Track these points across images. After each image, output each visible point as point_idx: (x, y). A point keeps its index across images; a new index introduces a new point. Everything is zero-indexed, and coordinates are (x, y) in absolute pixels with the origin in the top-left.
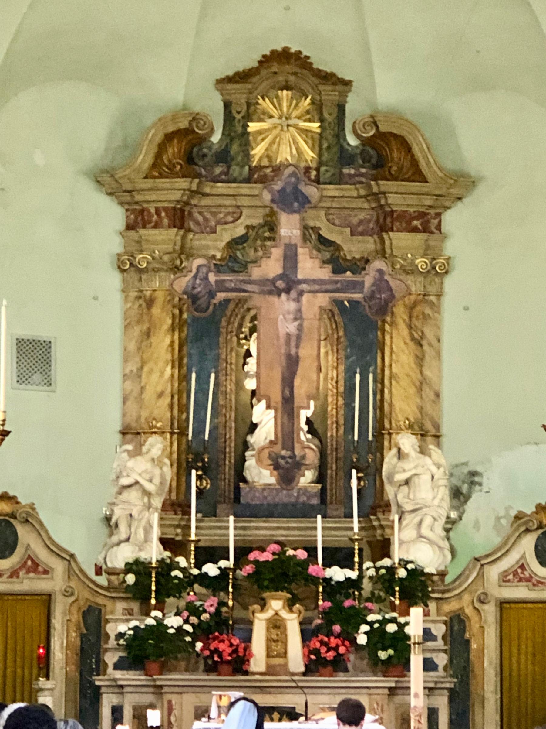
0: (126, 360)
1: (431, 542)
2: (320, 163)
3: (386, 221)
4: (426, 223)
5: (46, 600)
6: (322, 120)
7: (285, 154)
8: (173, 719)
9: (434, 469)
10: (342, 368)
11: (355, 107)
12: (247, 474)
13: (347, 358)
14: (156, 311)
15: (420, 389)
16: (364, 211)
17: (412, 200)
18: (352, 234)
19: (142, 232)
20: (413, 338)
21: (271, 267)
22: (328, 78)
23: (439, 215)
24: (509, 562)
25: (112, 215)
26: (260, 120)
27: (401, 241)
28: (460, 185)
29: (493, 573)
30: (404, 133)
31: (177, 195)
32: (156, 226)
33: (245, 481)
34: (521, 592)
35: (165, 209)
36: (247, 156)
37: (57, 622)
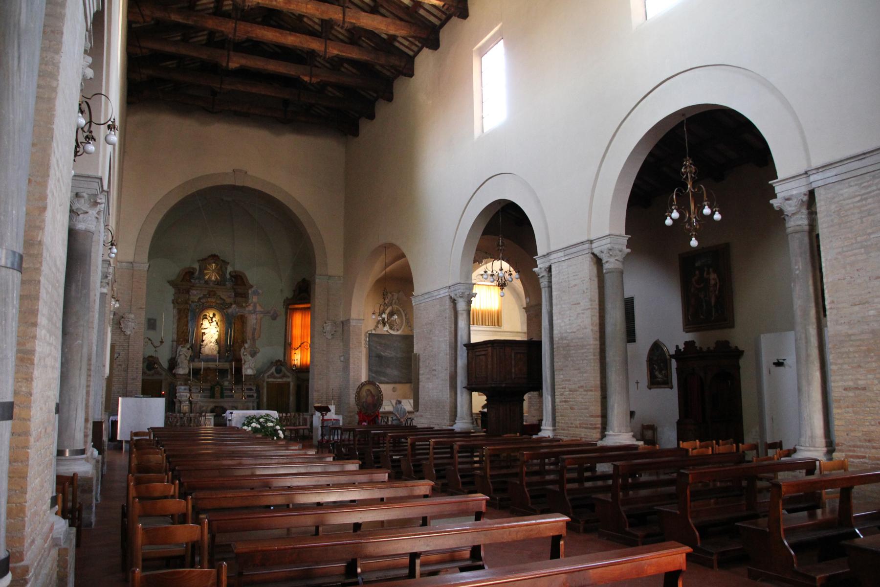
5: (161, 382)
11: (230, 269)
21: (251, 308)
22: (223, 261)
25: (170, 292)
29: (266, 375)
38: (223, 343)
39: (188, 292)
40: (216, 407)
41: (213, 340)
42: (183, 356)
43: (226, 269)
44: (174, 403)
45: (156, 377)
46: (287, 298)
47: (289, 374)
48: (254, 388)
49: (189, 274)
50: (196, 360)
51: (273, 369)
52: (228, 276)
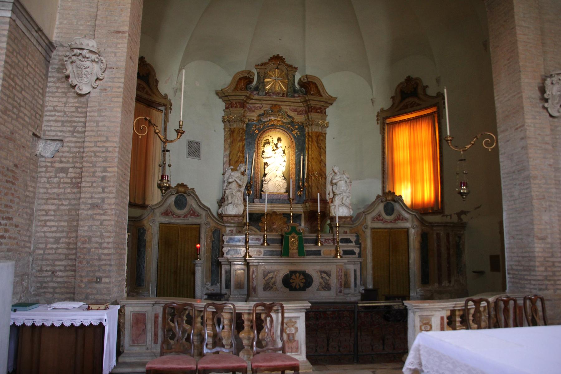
0: (225, 151)
1: (346, 206)
2: (288, 92)
3: (309, 109)
4: (321, 111)
5: (198, 228)
6: (288, 79)
7: (277, 89)
8: (254, 276)
9: (346, 179)
10: (294, 156)
11: (298, 76)
12: (264, 189)
13: (296, 153)
14: (235, 134)
15: (320, 163)
17: (318, 103)
18: (298, 114)
19: (231, 109)
20: (318, 146)
22: (291, 66)
23: (325, 109)
24: (374, 214)
25: (221, 105)
26: (268, 78)
27: (313, 115)
28: (330, 101)
29: (369, 218)
30: (316, 82)
31: (243, 98)
32: (236, 107)
33: (263, 191)
35: (239, 102)
36: (264, 88)
38: (293, 176)
39: (243, 105)
40: (292, 273)
41: (280, 173)
42: (234, 185)
43: (294, 76)
44: (219, 265)
45: (191, 220)
46: (382, 110)
47: (406, 215)
48: (353, 239)
49: (244, 81)
50: (256, 200)
51: (381, 207)
52: (297, 86)
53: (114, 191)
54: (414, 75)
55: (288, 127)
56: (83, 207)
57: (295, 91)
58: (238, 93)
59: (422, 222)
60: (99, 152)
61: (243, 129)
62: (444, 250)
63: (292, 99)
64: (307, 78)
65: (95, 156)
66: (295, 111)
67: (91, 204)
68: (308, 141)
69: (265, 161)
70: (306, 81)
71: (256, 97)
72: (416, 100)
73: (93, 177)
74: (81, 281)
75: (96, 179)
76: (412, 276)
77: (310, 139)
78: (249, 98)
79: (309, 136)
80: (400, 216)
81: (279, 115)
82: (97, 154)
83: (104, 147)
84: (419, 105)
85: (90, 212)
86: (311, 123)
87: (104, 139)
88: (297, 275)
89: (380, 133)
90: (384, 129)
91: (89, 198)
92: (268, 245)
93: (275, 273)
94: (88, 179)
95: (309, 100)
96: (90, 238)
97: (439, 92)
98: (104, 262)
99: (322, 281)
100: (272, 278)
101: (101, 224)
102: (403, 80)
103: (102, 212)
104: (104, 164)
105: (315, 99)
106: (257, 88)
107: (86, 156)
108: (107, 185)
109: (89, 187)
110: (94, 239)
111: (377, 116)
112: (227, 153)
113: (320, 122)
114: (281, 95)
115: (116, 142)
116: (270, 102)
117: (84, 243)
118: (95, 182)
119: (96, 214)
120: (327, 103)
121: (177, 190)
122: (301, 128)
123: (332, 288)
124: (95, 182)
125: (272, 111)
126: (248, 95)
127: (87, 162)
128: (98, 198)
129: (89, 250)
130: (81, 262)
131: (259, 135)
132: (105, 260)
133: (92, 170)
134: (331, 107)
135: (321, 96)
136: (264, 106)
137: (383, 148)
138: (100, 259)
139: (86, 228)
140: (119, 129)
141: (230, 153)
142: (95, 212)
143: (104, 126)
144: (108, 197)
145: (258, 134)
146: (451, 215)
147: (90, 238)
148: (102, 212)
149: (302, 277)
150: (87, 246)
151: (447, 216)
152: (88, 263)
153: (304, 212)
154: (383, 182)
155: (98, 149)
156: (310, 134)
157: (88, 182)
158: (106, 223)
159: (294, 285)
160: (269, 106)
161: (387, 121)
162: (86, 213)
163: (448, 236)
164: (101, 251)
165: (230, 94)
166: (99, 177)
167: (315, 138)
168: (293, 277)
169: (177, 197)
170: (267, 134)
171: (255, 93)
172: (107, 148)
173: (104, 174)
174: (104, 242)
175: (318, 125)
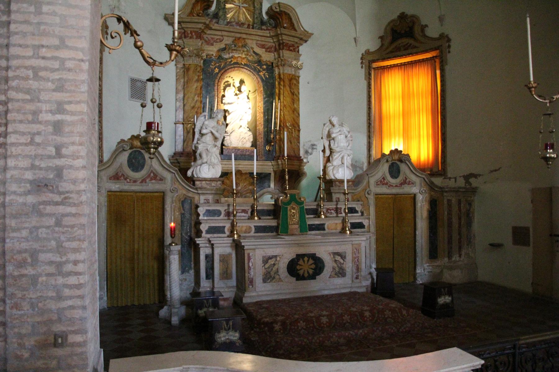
0: (177, 92)
2: (254, 23)
3: (280, 46)
4: (294, 49)
5: (162, 197)
6: (254, 7)
8: (251, 264)
9: (347, 133)
10: (262, 102)
13: (264, 98)
14: (191, 72)
15: (294, 112)
16: (270, 42)
17: (291, 39)
18: (266, 51)
19: (185, 40)
23: (298, 47)
26: (230, 4)
27: (286, 54)
28: (305, 37)
30: (289, 12)
31: (200, 26)
32: (191, 38)
34: (384, 190)
35: (194, 32)
36: (225, 16)
37: (168, 207)
38: (261, 128)
40: (300, 257)
41: (245, 125)
45: (152, 186)
46: (368, 52)
47: (413, 178)
53: (83, 153)
54: (410, 11)
55: (255, 66)
56: (13, 187)
57: (262, 23)
58: (196, 19)
59: (432, 187)
60: (46, 69)
61: (200, 66)
62: (455, 220)
63: (260, 33)
64: (279, 6)
65: (36, 77)
66: (263, 46)
67: (31, 182)
68: (279, 84)
69: (226, 107)
70: (278, 10)
71: (216, 26)
72: (411, 41)
73: (33, 122)
74: (21, 346)
75: (41, 128)
76: (418, 250)
77: (282, 83)
78: (208, 27)
79: (280, 78)
80: (406, 179)
81: (243, 51)
82: (42, 74)
83: (54, 58)
84: (415, 47)
85: (31, 199)
86: (283, 63)
87: (56, 42)
88: (306, 259)
89: (365, 79)
90: (370, 74)
91: (26, 169)
92: (260, 219)
93: (278, 259)
94: (22, 127)
95: (281, 34)
96: (34, 254)
97: (443, 33)
98: (70, 303)
99: (336, 265)
100: (274, 264)
101: (58, 223)
102: (395, 16)
103: (57, 198)
104: (58, 96)
105: (289, 34)
106: (216, 16)
107: (17, 77)
108: (65, 140)
109: (26, 144)
110: (43, 257)
111: (362, 59)
112: (181, 95)
113: (294, 62)
114: (246, 26)
115: (82, 50)
116: (233, 34)
117: (22, 264)
118: (39, 133)
119: (45, 203)
120: (301, 39)
121: (132, 144)
122: (270, 68)
123: (347, 273)
124: (39, 133)
125: (235, 46)
126: (207, 22)
127: (18, 89)
128: (48, 169)
129: (34, 280)
130: (16, 306)
131: (219, 75)
132: (71, 298)
133: (30, 107)
134: (305, 44)
135: (295, 30)
136: (225, 38)
137: (369, 97)
138: (60, 298)
139: (25, 233)
140: (87, 23)
141: (184, 97)
142: (43, 198)
143: (54, 14)
144: (71, 167)
145: (218, 73)
146: (455, 178)
147: (34, 254)
148: (57, 198)
149: (311, 261)
150: (30, 271)
151: (450, 178)
152: (32, 306)
153: (275, 172)
154: (369, 137)
155: (42, 63)
156: (282, 76)
157: (23, 134)
158: (67, 221)
159: (301, 272)
160: (231, 39)
161: (373, 65)
162: (21, 200)
163: (459, 202)
164: (60, 280)
165: (184, 20)
166: (47, 123)
167: (287, 82)
168: (301, 262)
169: (130, 154)
170: (228, 75)
171: (214, 21)
172: (63, 61)
173: (59, 117)
174: (67, 262)
175: (291, 66)
